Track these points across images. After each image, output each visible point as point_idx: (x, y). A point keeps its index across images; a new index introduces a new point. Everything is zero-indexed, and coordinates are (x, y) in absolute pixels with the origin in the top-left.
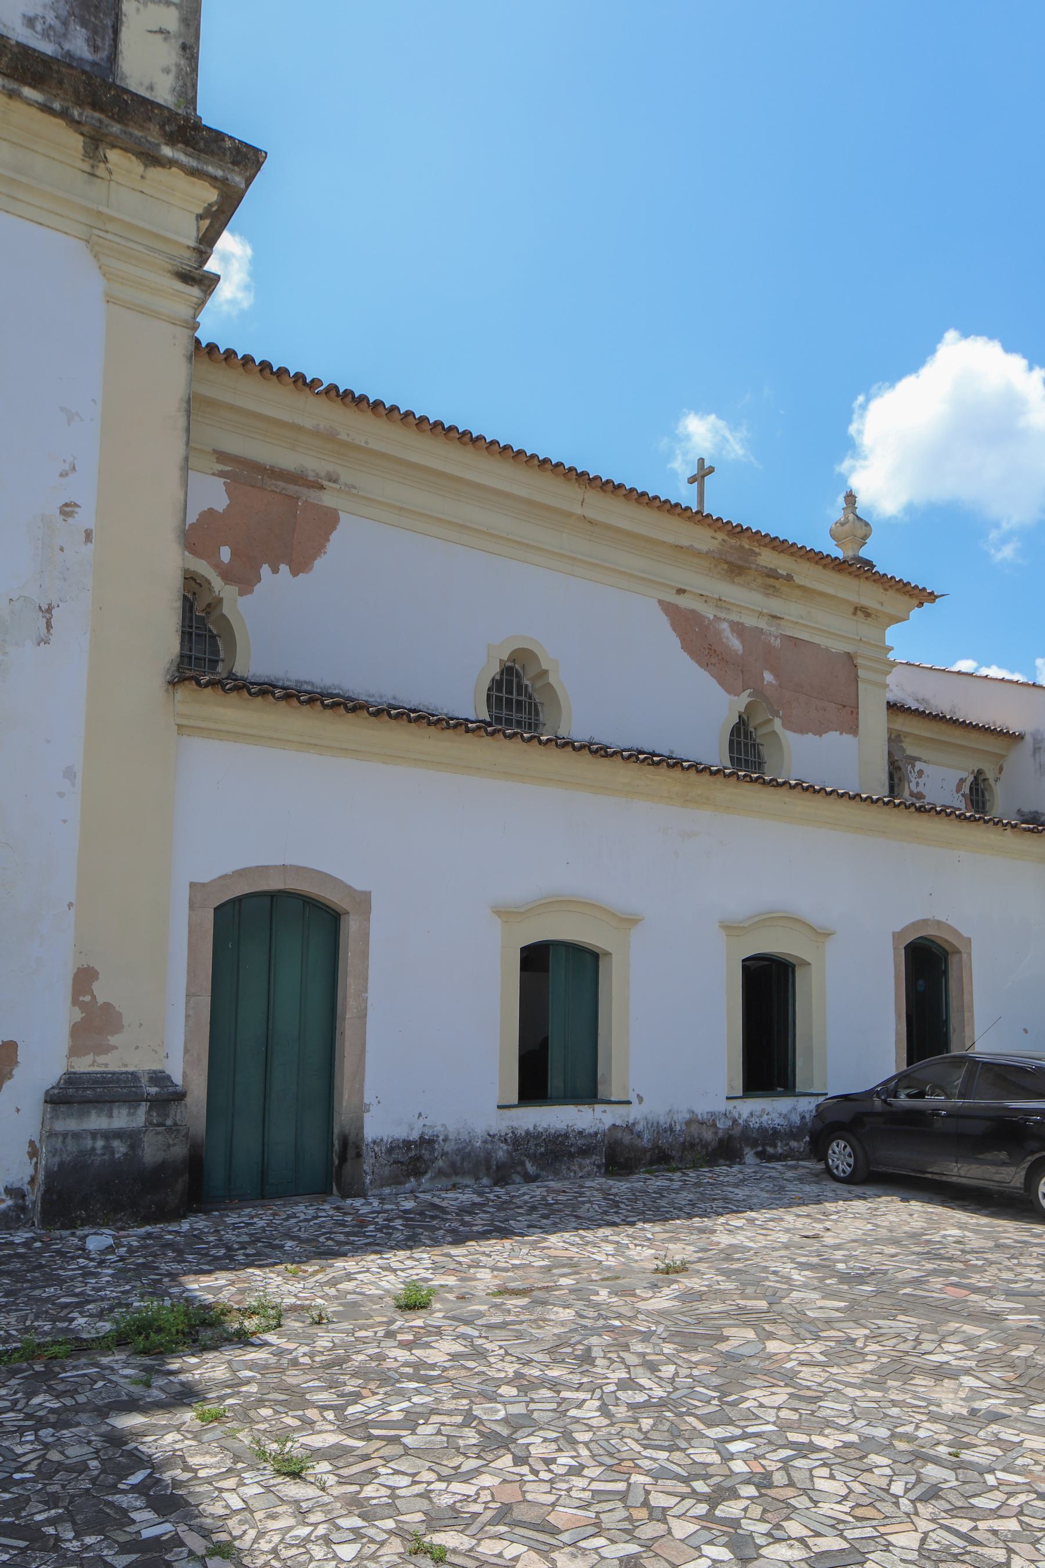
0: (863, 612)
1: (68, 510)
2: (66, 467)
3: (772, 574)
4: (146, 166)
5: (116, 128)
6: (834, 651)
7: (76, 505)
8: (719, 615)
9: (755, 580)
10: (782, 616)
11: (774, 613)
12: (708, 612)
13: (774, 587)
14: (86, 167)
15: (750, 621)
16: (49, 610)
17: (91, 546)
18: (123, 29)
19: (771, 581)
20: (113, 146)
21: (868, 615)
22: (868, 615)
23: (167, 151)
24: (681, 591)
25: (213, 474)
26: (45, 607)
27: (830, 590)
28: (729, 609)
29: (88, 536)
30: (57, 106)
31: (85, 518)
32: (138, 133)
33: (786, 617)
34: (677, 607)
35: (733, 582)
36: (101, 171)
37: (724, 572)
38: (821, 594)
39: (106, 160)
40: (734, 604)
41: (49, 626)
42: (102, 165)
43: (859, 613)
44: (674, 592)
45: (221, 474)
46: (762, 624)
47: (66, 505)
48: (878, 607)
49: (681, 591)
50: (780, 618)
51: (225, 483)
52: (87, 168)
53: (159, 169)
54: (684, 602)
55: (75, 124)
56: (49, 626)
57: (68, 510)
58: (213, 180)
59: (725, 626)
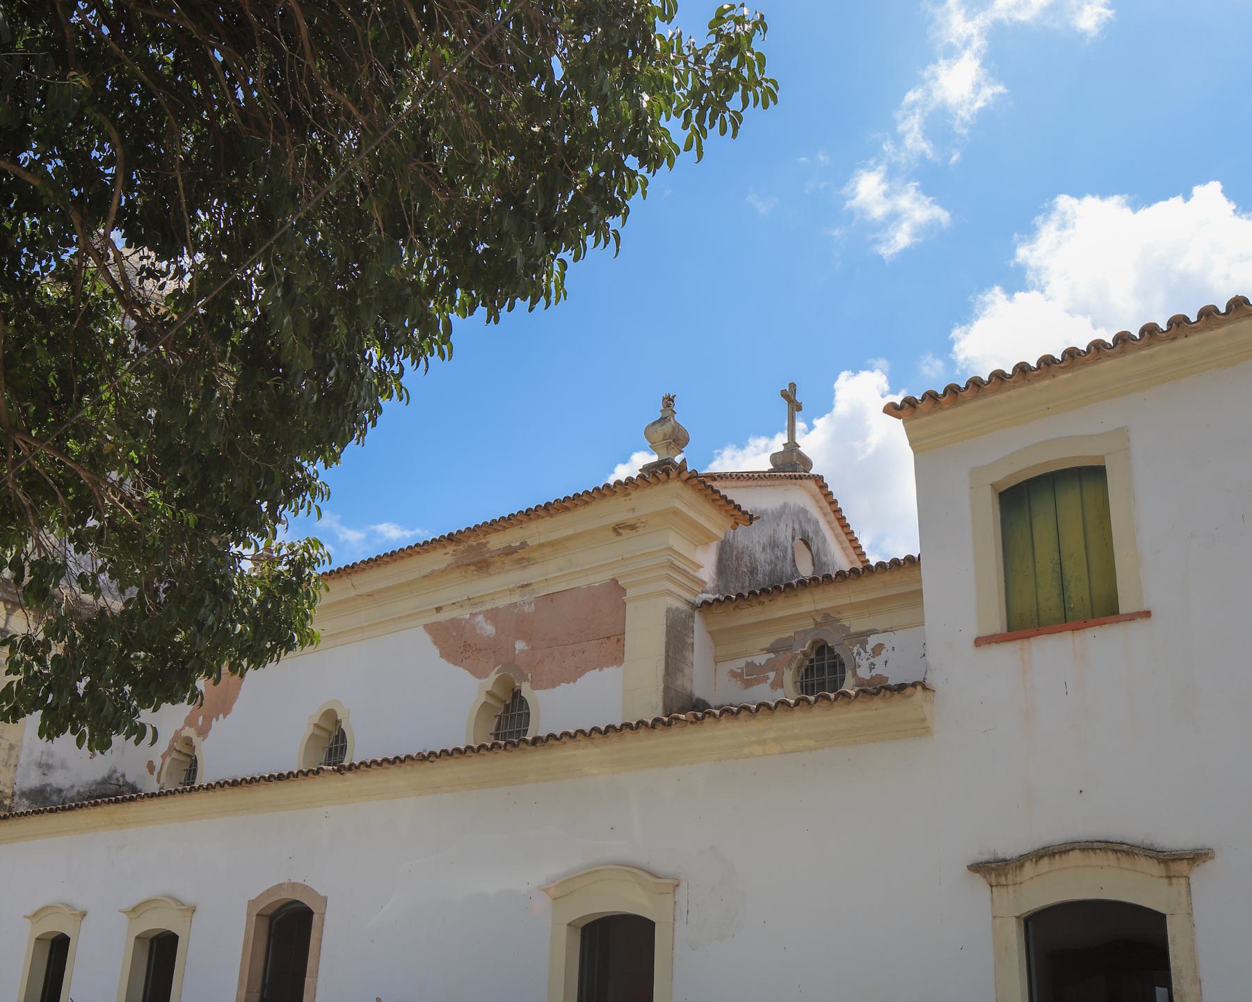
0: (624, 528)
3: (509, 551)
6: (597, 585)
8: (474, 611)
9: (504, 563)
10: (529, 582)
11: (521, 583)
12: (464, 614)
13: (523, 558)
15: (502, 602)
19: (515, 556)
21: (632, 527)
22: (632, 527)
24: (439, 609)
27: (570, 532)
28: (483, 602)
33: (532, 581)
34: (439, 623)
35: (490, 575)
37: (476, 572)
38: (568, 538)
40: (482, 596)
43: (620, 531)
44: (435, 612)
46: (516, 598)
48: (630, 515)
49: (439, 609)
50: (528, 585)
54: (443, 617)
59: (480, 618)
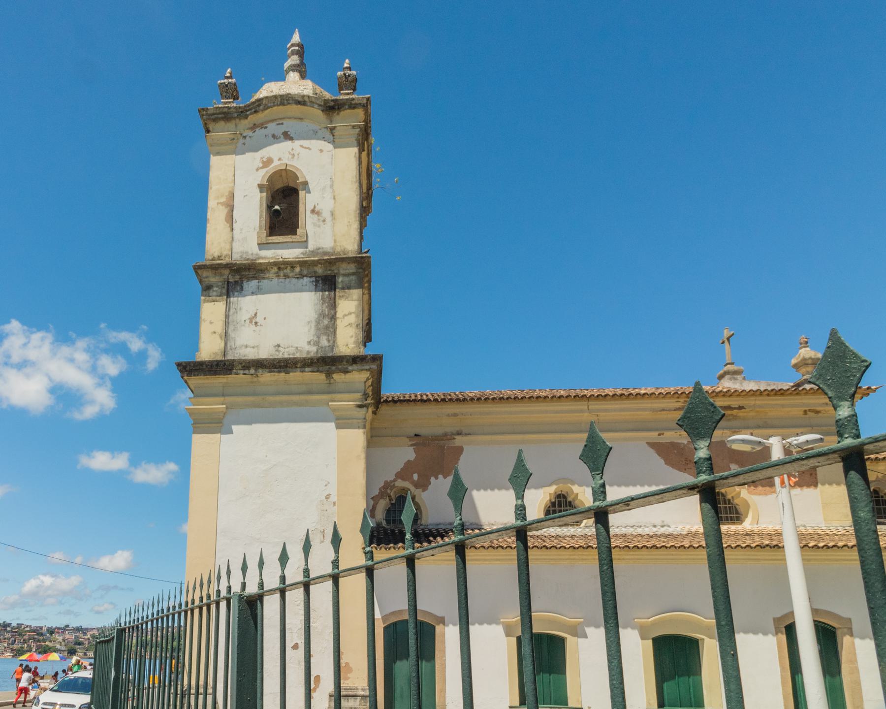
1: (328, 497)
2: (326, 483)
4: (345, 375)
5: (333, 368)
7: (330, 495)
14: (328, 382)
16: (324, 532)
17: (336, 507)
18: (337, 330)
20: (334, 373)
23: (350, 368)
25: (409, 446)
26: (322, 531)
29: (334, 503)
30: (315, 370)
31: (334, 498)
32: (340, 367)
36: (332, 381)
39: (333, 378)
41: (324, 536)
42: (332, 380)
45: (412, 445)
47: (327, 495)
51: (414, 448)
52: (329, 382)
53: (349, 374)
55: (321, 372)
56: (324, 536)
57: (328, 497)
58: (367, 370)
